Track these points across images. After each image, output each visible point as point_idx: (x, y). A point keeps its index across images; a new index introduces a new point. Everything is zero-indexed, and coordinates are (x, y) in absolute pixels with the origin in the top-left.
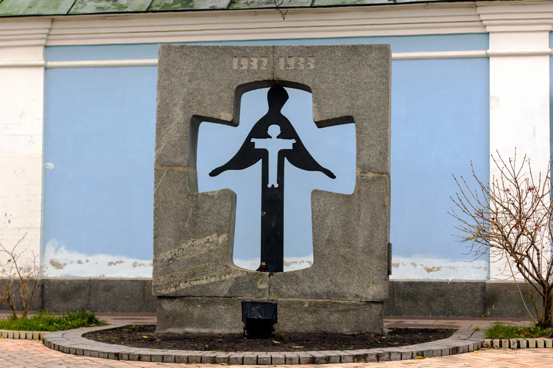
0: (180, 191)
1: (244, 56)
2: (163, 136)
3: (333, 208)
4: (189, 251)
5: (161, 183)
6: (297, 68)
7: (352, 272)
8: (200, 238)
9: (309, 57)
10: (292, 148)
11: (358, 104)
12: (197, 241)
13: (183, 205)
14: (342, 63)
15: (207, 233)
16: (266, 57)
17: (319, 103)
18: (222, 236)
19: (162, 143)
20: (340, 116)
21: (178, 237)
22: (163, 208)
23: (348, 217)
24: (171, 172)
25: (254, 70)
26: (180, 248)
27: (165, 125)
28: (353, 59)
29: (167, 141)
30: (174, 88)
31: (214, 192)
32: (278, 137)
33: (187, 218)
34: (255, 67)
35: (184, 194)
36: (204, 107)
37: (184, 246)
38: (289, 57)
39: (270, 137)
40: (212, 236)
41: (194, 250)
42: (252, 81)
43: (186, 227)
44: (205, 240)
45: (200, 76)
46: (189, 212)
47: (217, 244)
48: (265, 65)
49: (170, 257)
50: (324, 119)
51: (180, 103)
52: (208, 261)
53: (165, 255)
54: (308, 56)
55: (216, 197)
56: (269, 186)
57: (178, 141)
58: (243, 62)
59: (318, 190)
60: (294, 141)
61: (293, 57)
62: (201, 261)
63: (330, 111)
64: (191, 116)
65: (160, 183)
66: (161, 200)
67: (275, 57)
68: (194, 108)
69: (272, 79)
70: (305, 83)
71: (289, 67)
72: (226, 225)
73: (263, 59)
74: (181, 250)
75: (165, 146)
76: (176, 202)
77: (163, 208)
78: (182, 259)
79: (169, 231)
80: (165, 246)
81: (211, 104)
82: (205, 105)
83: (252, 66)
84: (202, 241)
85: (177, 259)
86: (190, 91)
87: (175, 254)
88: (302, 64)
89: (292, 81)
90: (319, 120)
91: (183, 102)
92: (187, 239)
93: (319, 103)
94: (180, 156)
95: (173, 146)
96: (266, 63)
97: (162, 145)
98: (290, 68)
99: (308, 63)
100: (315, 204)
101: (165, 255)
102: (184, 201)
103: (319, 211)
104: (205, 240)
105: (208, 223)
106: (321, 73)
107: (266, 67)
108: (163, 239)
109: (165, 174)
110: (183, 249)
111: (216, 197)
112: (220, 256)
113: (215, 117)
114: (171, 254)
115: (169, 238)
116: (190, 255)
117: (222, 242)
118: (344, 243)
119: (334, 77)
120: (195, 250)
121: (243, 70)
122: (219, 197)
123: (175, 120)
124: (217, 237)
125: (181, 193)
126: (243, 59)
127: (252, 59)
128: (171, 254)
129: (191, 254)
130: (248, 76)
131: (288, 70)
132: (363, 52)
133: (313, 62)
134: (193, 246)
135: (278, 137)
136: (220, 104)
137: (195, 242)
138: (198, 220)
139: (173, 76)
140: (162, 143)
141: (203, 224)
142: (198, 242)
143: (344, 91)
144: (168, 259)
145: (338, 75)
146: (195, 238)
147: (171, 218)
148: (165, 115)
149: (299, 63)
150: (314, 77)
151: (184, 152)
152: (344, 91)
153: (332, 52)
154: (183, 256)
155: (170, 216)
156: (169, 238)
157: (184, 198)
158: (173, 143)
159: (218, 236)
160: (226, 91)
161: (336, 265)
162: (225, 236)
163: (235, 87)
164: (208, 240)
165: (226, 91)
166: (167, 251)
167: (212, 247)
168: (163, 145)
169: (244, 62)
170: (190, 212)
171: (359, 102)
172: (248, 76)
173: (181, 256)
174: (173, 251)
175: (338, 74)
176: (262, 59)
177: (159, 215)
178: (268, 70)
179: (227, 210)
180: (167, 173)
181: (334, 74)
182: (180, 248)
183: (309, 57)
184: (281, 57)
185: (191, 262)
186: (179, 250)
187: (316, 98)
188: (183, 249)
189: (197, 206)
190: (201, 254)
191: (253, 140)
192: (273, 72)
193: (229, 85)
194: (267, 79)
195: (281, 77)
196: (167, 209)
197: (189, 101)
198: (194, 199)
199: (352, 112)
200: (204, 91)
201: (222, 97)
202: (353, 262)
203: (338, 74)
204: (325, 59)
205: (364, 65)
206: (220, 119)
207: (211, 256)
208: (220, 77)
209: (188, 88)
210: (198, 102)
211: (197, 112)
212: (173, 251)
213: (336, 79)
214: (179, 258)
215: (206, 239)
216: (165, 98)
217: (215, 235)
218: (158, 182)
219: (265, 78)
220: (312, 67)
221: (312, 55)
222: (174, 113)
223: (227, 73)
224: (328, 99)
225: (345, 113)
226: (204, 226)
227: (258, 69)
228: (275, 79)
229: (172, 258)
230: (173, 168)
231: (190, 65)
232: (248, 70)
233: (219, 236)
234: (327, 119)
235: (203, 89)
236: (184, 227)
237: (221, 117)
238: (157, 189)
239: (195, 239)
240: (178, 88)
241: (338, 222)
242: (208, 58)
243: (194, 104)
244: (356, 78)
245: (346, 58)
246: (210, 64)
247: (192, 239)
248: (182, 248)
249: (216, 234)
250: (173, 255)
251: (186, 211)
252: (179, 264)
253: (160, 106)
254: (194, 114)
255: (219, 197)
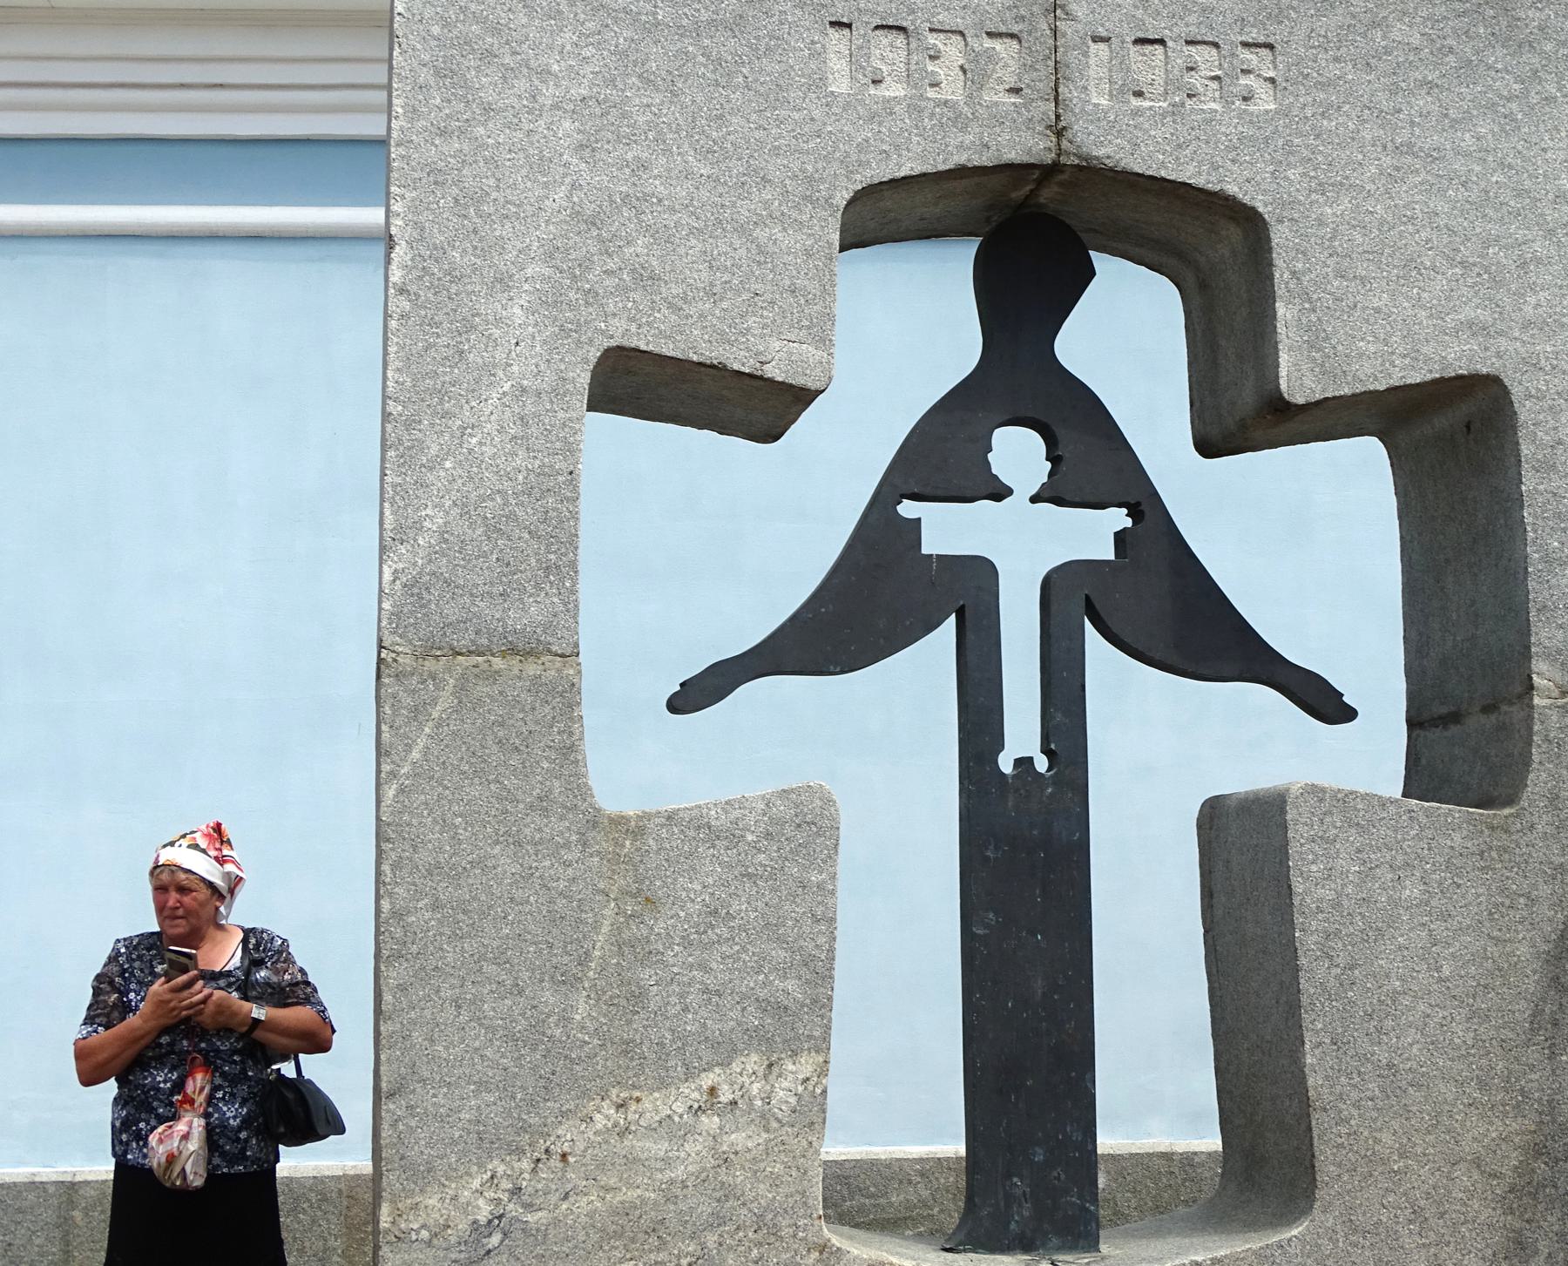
0: (540, 798)
1: (891, 22)
2: (431, 469)
3: (1411, 891)
4: (601, 1166)
5: (426, 751)
6: (1183, 105)
7: (1536, 1252)
8: (662, 1084)
9: (1245, 45)
10: (1110, 555)
11: (1528, 309)
12: (647, 1104)
13: (562, 884)
14: (1430, 86)
15: (707, 1056)
16: (1012, 36)
17: (1310, 301)
18: (791, 1067)
19: (429, 511)
20: (1429, 377)
21: (531, 1082)
22: (436, 906)
23: (1497, 941)
24: (483, 689)
25: (946, 102)
26: (547, 1151)
27: (441, 402)
28: (1489, 68)
29: (454, 495)
30: (492, 182)
31: (742, 802)
32: (1035, 499)
33: (583, 962)
34: (953, 89)
35: (562, 818)
36: (671, 306)
37: (568, 1135)
38: (1140, 41)
39: (999, 492)
40: (736, 1067)
41: (632, 1161)
42: (942, 167)
43: (578, 1017)
44: (692, 1093)
45: (641, 119)
46: (596, 927)
47: (763, 1116)
48: (1011, 81)
49: (484, 1212)
50: (1346, 391)
51: (529, 272)
52: (718, 1220)
53: (455, 1198)
54: (1240, 39)
55: (750, 838)
56: (1006, 764)
57: (525, 498)
58: (882, 58)
59: (1323, 790)
60: (1118, 518)
61: (1161, 42)
62: (673, 1224)
63: (1372, 348)
64: (594, 354)
65: (415, 755)
66: (424, 857)
67: (1064, 34)
68: (611, 308)
69: (1049, 158)
70: (1232, 189)
71: (1139, 94)
72: (814, 1002)
73: (998, 45)
74: (555, 1162)
75: (442, 533)
76: (516, 868)
77: (436, 906)
78: (556, 1222)
79: (477, 1049)
80: (454, 1142)
81: (712, 285)
82: (676, 290)
83: (934, 85)
84: (678, 1102)
85: (529, 1218)
86: (590, 208)
87: (516, 1191)
88: (1214, 85)
89: (1163, 174)
90: (1318, 397)
91: (547, 271)
92: (585, 1094)
93: (1310, 301)
94: (537, 586)
95: (492, 530)
96: (1014, 66)
97: (427, 524)
98: (1147, 104)
99: (1241, 82)
100: (1314, 868)
101: (455, 1198)
102: (566, 864)
103: (1337, 905)
104: (692, 1093)
105: (706, 991)
106: (1317, 136)
107: (1016, 91)
108: (441, 1100)
109: (446, 700)
110: (564, 1156)
111: (750, 838)
112: (783, 1190)
113: (736, 367)
114: (490, 1194)
115: (476, 1093)
116: (608, 1189)
117: (793, 1100)
118: (1483, 1085)
119: (1387, 161)
120: (636, 1160)
121: (887, 100)
122: (768, 835)
123: (500, 373)
124: (766, 1077)
125: (545, 812)
126: (885, 41)
127: (932, 39)
128: (490, 1194)
129: (613, 1182)
130: (915, 139)
131: (1137, 112)
132: (1540, 28)
133: (1271, 74)
134: (624, 1132)
135: (1035, 499)
136: (759, 287)
137: (633, 1107)
138: (647, 975)
139: (487, 109)
140: (429, 511)
141: (682, 996)
142: (654, 1106)
143: (1446, 239)
144: (475, 1222)
145: (1408, 148)
146: (634, 1087)
147: (489, 969)
148: (443, 341)
149: (1195, 80)
150: (1278, 156)
151: (557, 567)
152: (1446, 239)
153: (1375, 25)
154: (566, 1197)
155: (483, 958)
156: (476, 1093)
157: (567, 845)
158: (491, 508)
159: (770, 1066)
160: (795, 214)
161: (1442, 1215)
162: (806, 1065)
163: (842, 197)
164: (713, 1091)
165: (795, 214)
166: (469, 1174)
167: (738, 1139)
168: (434, 520)
169: (888, 52)
170: (605, 929)
171: (1532, 300)
172: (915, 139)
173: (554, 1198)
174: (501, 1169)
175: (1410, 145)
176: (988, 43)
177: (414, 949)
178: (1025, 105)
179: (819, 911)
180: (461, 688)
181: (1389, 145)
182: (547, 1151)
183: (1245, 45)
184: (1097, 39)
185: (618, 1235)
186: (538, 1160)
187: (1294, 273)
188: (564, 1156)
189: (639, 890)
190: (672, 1182)
191: (907, 509)
192: (1058, 117)
193: (810, 180)
194: (1026, 159)
195: (1101, 152)
196: (465, 912)
197: (586, 264)
198: (623, 846)
199: (1499, 355)
200: (673, 210)
201: (771, 248)
202: (1541, 1197)
203: (1410, 145)
204: (1336, 60)
205: (1550, 100)
206: (761, 378)
207: (728, 1193)
208: (758, 134)
209: (574, 186)
210: (634, 271)
211: (633, 328)
212: (501, 1169)
213: (1397, 169)
214: (540, 1214)
215: (699, 1088)
216: (439, 239)
217: (754, 1061)
218: (409, 748)
219: (1012, 155)
220: (1265, 102)
221: (1262, 39)
222: (496, 333)
223: (796, 115)
224: (1363, 280)
225: (1460, 359)
226: (686, 1009)
227: (970, 96)
228: (1063, 159)
229: (500, 1217)
230: (498, 663)
231: (587, 52)
232: (915, 109)
233: (775, 1069)
234: (1360, 389)
235: (660, 201)
236: (565, 1020)
237: (766, 367)
238: (402, 790)
239: (637, 1094)
240: (514, 186)
241: (1446, 971)
242: (685, 22)
243: (610, 282)
244: (1510, 167)
245: (1451, 58)
246: (701, 59)
247: (614, 1092)
248: (557, 1149)
249: (754, 1057)
250: (505, 1197)
251: (580, 921)
252: (539, 1250)
253: (413, 288)
254: (613, 343)
255: (768, 835)
